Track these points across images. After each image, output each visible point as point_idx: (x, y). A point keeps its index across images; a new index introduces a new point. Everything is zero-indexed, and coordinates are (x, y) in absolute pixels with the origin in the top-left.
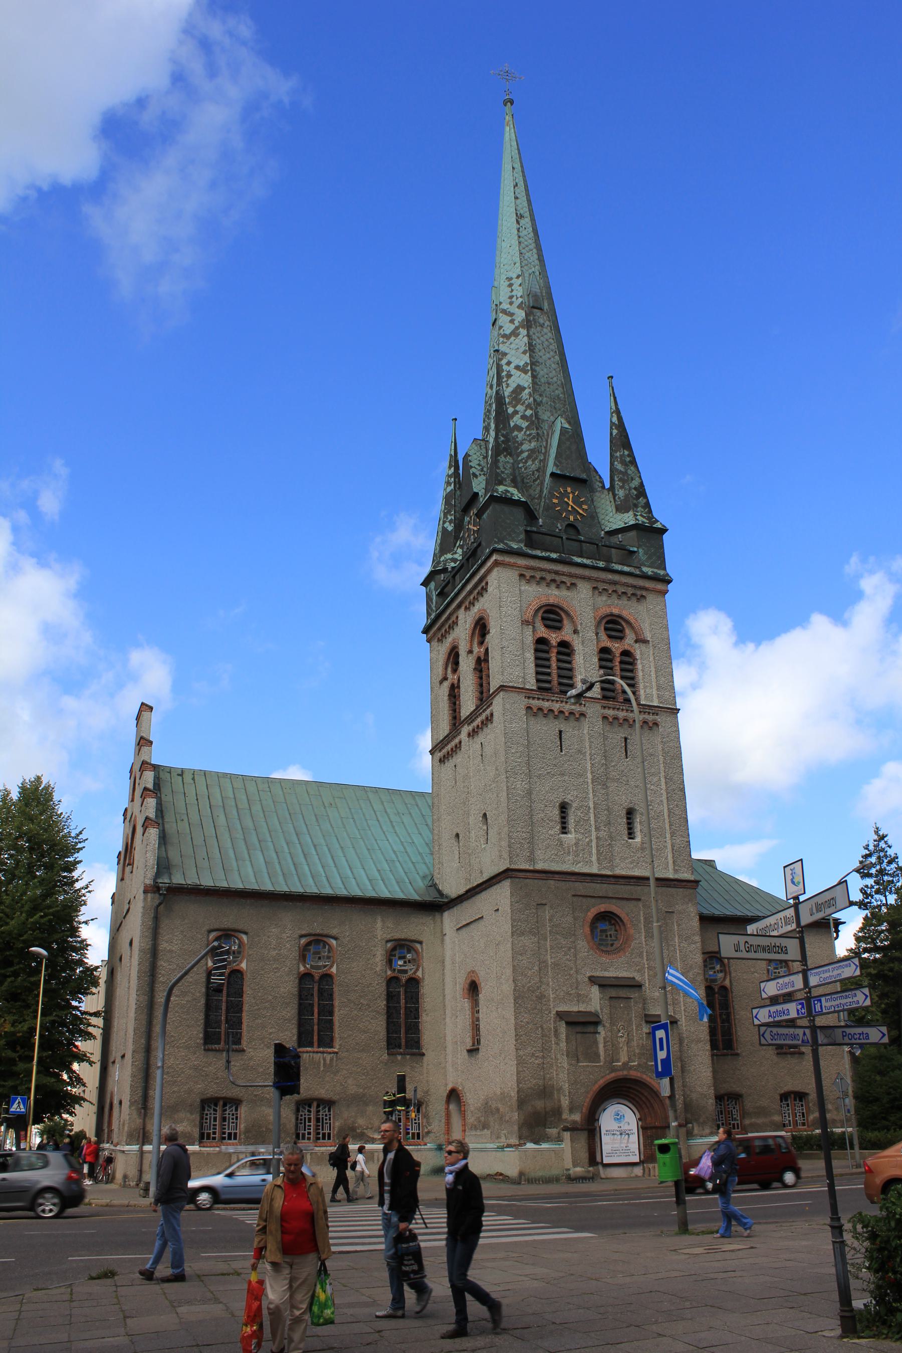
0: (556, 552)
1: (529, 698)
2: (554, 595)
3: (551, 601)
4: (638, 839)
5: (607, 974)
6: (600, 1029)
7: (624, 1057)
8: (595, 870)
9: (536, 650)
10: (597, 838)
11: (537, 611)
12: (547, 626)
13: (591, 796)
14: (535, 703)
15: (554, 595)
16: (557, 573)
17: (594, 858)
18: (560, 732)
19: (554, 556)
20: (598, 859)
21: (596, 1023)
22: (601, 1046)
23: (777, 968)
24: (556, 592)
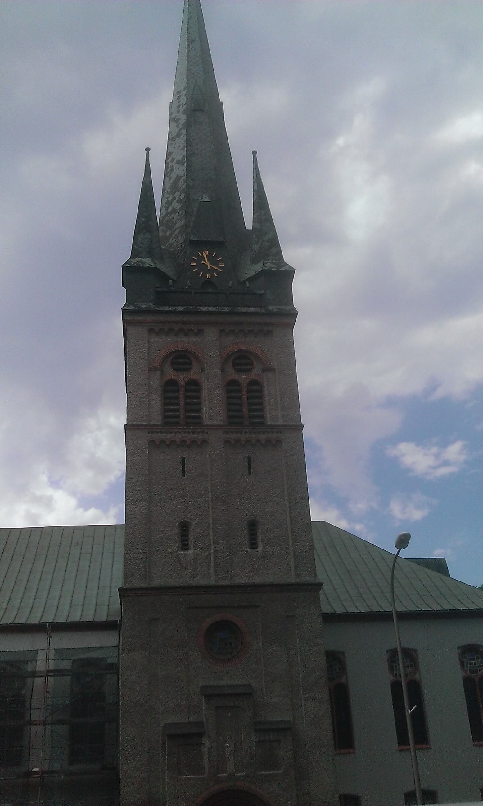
0: (182, 306)
1: (152, 433)
2: (182, 342)
3: (180, 347)
4: (260, 548)
5: (220, 683)
6: (205, 740)
7: (230, 767)
8: (212, 582)
9: (165, 391)
10: (215, 551)
11: (168, 356)
12: (176, 370)
13: (211, 513)
14: (158, 437)
15: (182, 342)
16: (183, 323)
17: (212, 571)
18: (183, 459)
19: (180, 309)
20: (216, 571)
21: (200, 735)
22: (206, 757)
23: (473, 660)
24: (185, 339)
